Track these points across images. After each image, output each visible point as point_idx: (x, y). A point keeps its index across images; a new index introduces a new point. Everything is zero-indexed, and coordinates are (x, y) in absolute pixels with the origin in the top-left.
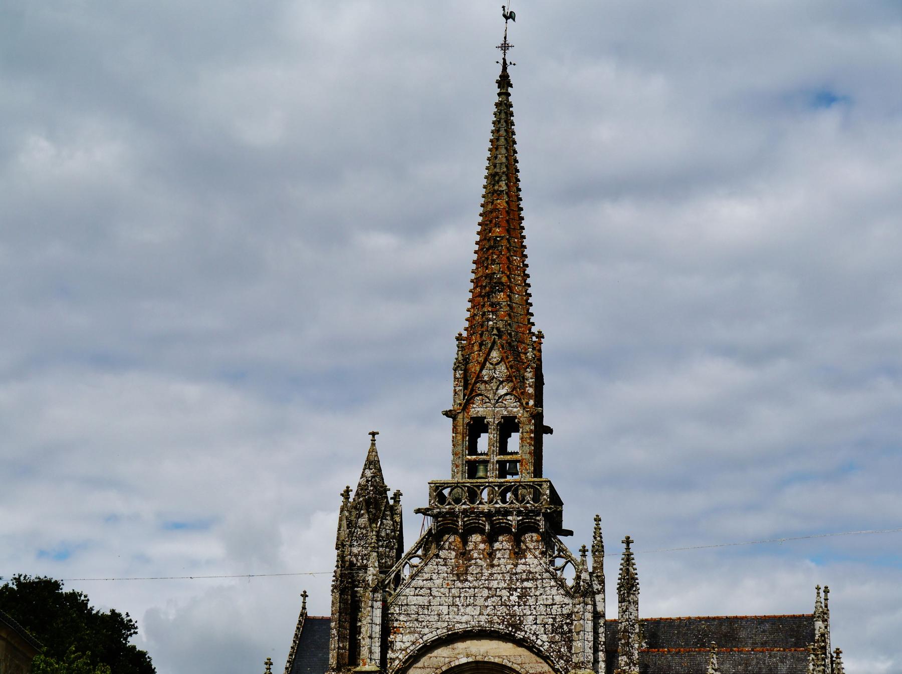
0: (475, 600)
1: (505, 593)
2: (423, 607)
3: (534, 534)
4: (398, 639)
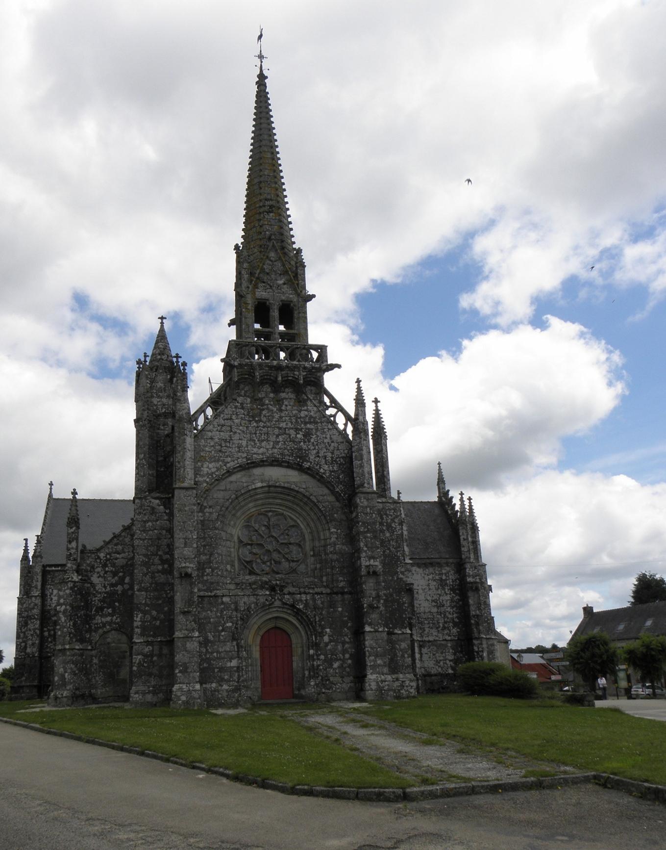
0: (268, 437)
1: (292, 432)
2: (225, 441)
3: (313, 388)
4: (205, 466)
